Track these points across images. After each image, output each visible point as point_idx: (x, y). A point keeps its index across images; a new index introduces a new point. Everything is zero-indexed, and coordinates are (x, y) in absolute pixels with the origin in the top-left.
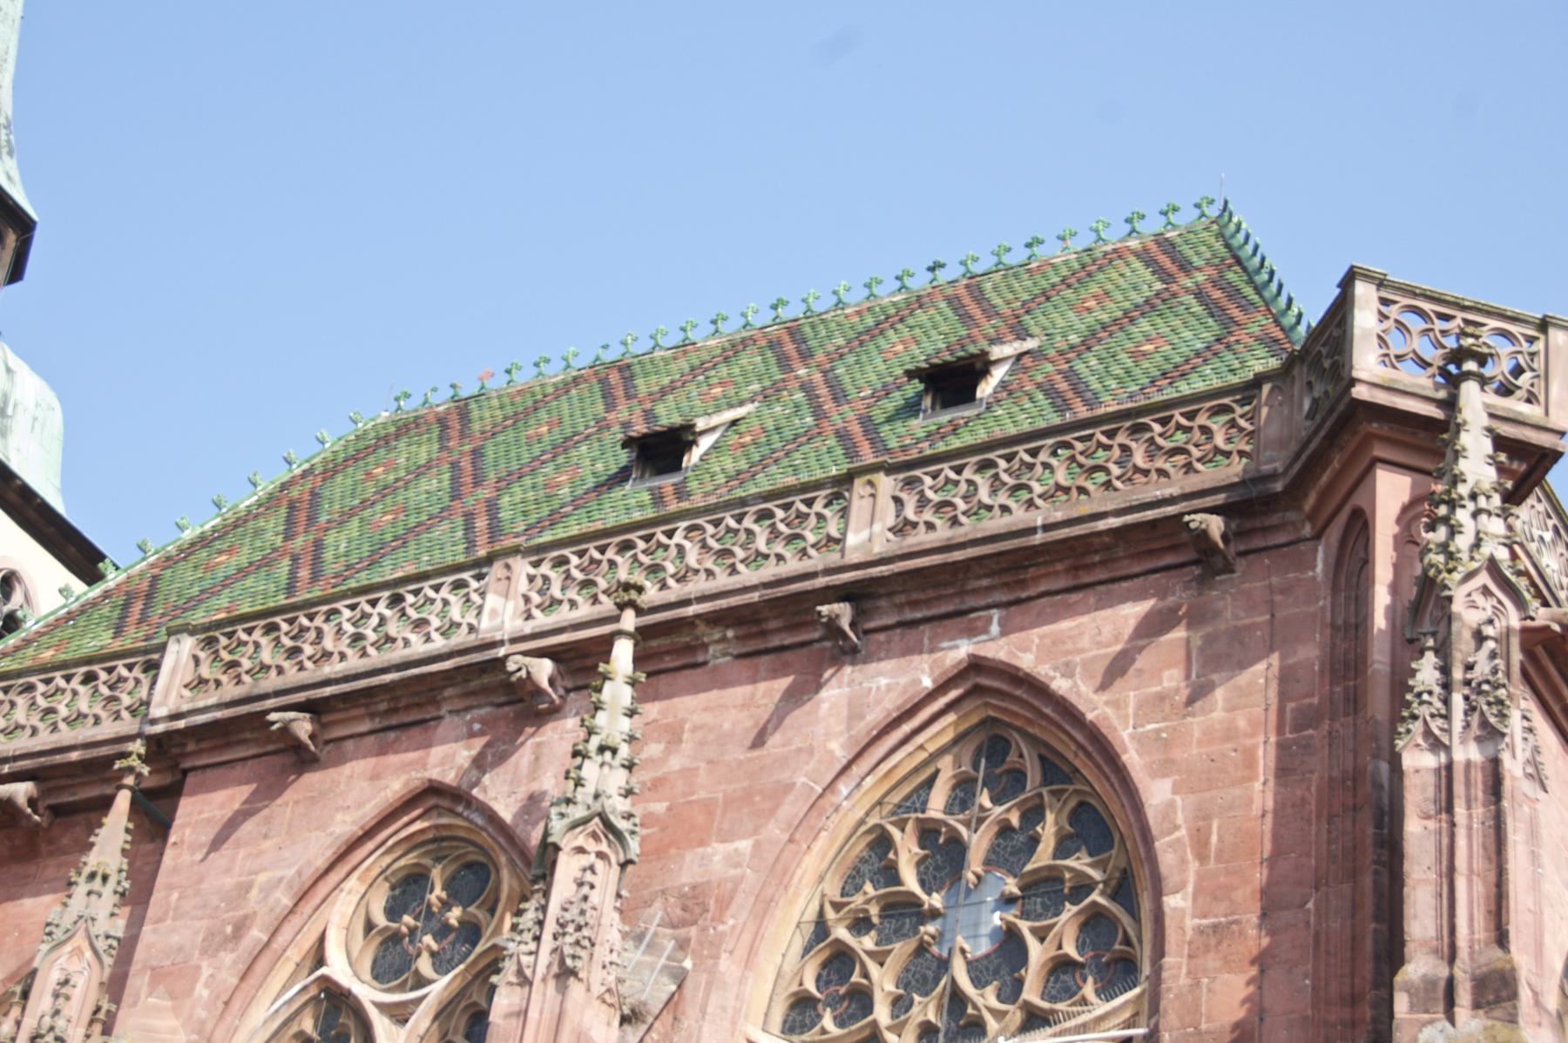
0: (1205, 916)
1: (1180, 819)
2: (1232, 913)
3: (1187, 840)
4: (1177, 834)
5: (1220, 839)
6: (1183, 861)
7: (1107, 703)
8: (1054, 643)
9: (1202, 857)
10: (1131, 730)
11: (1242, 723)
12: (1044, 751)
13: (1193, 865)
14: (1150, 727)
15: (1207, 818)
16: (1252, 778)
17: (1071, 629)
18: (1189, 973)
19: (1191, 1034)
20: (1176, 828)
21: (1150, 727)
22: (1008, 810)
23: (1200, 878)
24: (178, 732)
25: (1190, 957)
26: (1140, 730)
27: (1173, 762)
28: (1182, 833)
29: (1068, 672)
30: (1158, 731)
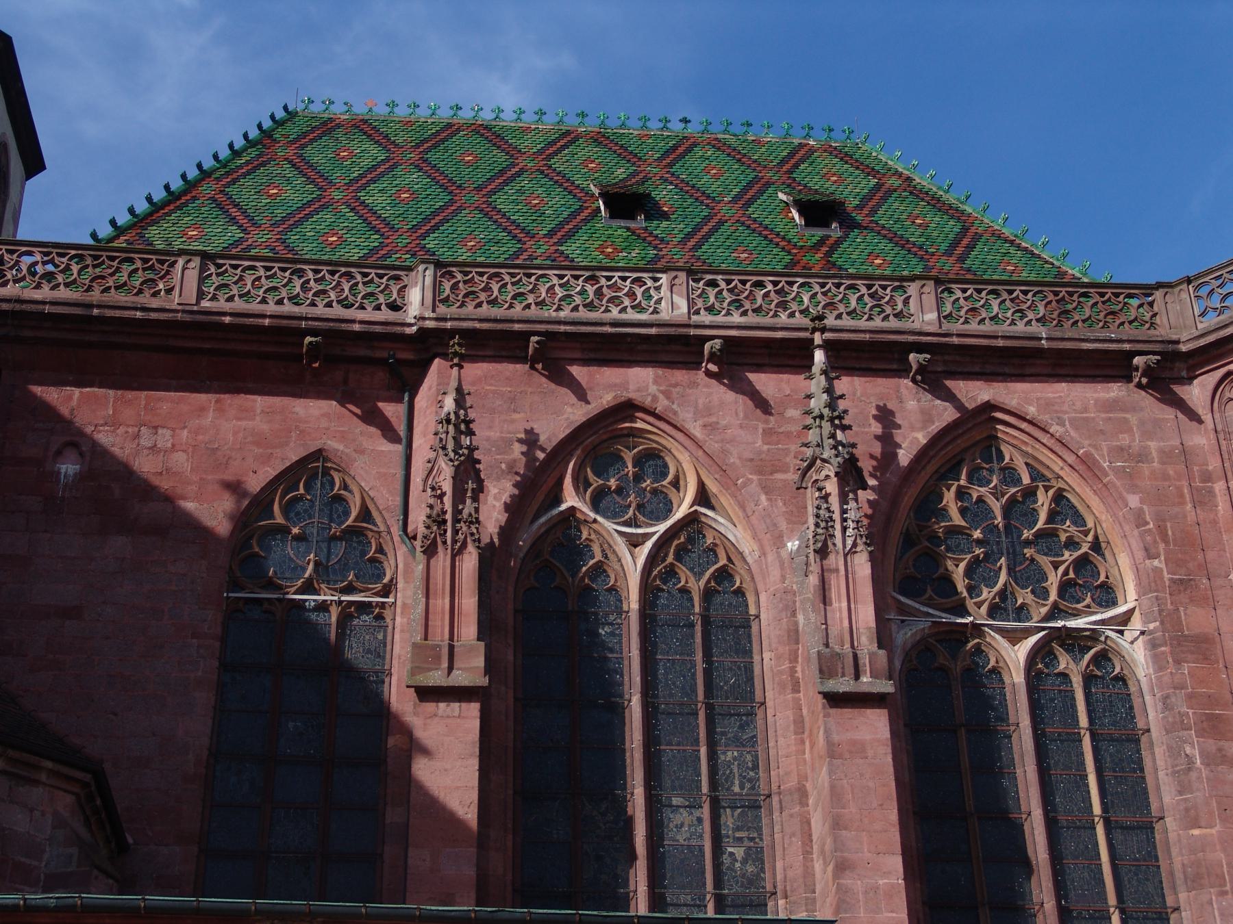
0: (1175, 575)
1: (1148, 518)
2: (1189, 575)
3: (1154, 530)
4: (1148, 527)
5: (1173, 533)
6: (1155, 542)
7: (1090, 445)
8: (1047, 404)
9: (1166, 542)
10: (1108, 464)
11: (1171, 472)
12: (1029, 461)
13: (1162, 546)
14: (1119, 464)
15: (1164, 521)
16: (1183, 503)
17: (1054, 398)
18: (1172, 603)
19: (1180, 636)
20: (1148, 523)
21: (1119, 464)
22: (1017, 492)
23: (1167, 553)
24: (445, 330)
25: (1170, 594)
26: (1113, 465)
27: (1137, 486)
28: (1151, 526)
29: (1062, 424)
30: (1123, 467)
